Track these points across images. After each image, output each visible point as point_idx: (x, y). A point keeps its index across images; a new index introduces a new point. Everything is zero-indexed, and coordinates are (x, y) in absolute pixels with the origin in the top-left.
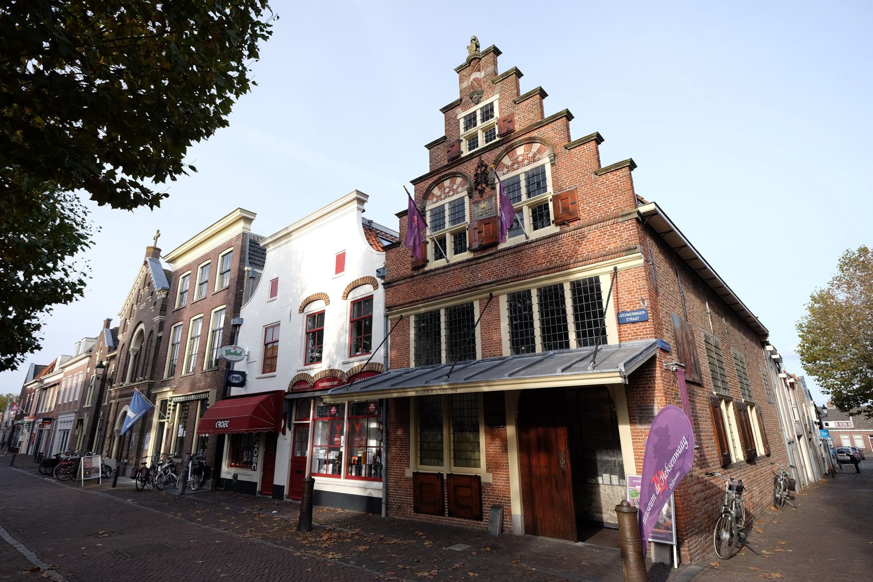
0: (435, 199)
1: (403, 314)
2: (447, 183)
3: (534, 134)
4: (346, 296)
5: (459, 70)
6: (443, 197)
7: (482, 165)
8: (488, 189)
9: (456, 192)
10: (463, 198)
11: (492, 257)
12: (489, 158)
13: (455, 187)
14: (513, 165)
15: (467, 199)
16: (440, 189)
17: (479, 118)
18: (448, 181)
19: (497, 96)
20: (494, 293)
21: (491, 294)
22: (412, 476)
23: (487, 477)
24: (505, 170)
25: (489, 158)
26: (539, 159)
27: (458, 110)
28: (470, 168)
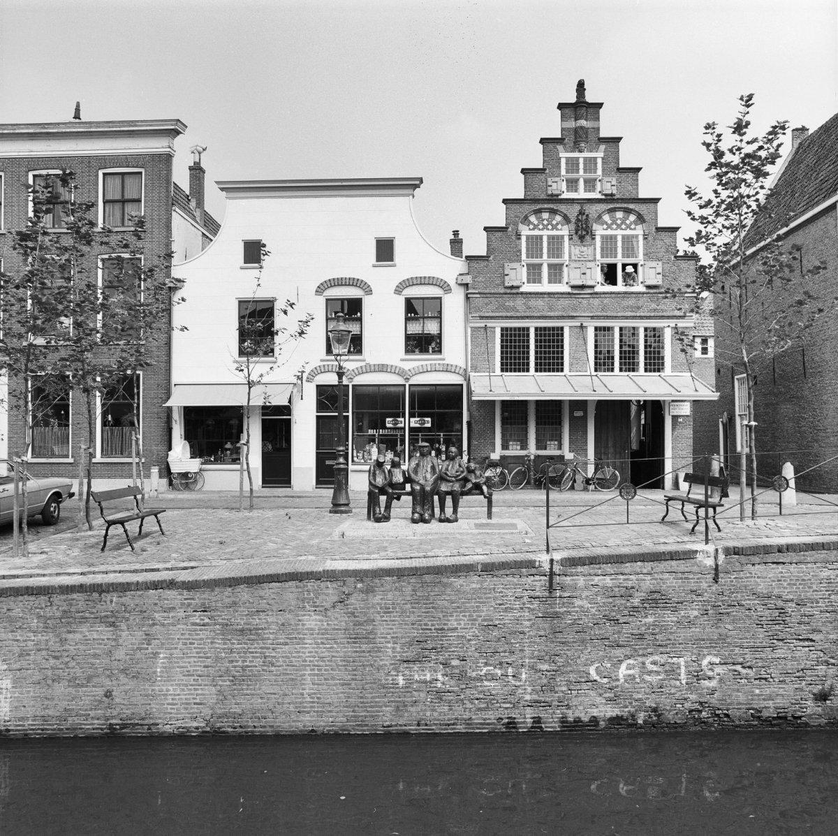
0: (531, 227)
1: (489, 325)
2: (545, 215)
3: (631, 206)
4: (398, 291)
5: (561, 106)
6: (541, 227)
7: (581, 213)
8: (588, 237)
9: (554, 227)
10: (562, 237)
11: (589, 296)
12: (593, 210)
13: (554, 222)
14: (612, 224)
15: (566, 239)
16: (537, 219)
17: (581, 166)
18: (548, 214)
19: (602, 155)
20: (584, 324)
21: (582, 324)
22: (499, 458)
23: (569, 456)
24: (605, 226)
25: (593, 210)
26: (635, 229)
27: (560, 148)
28: (573, 211)
